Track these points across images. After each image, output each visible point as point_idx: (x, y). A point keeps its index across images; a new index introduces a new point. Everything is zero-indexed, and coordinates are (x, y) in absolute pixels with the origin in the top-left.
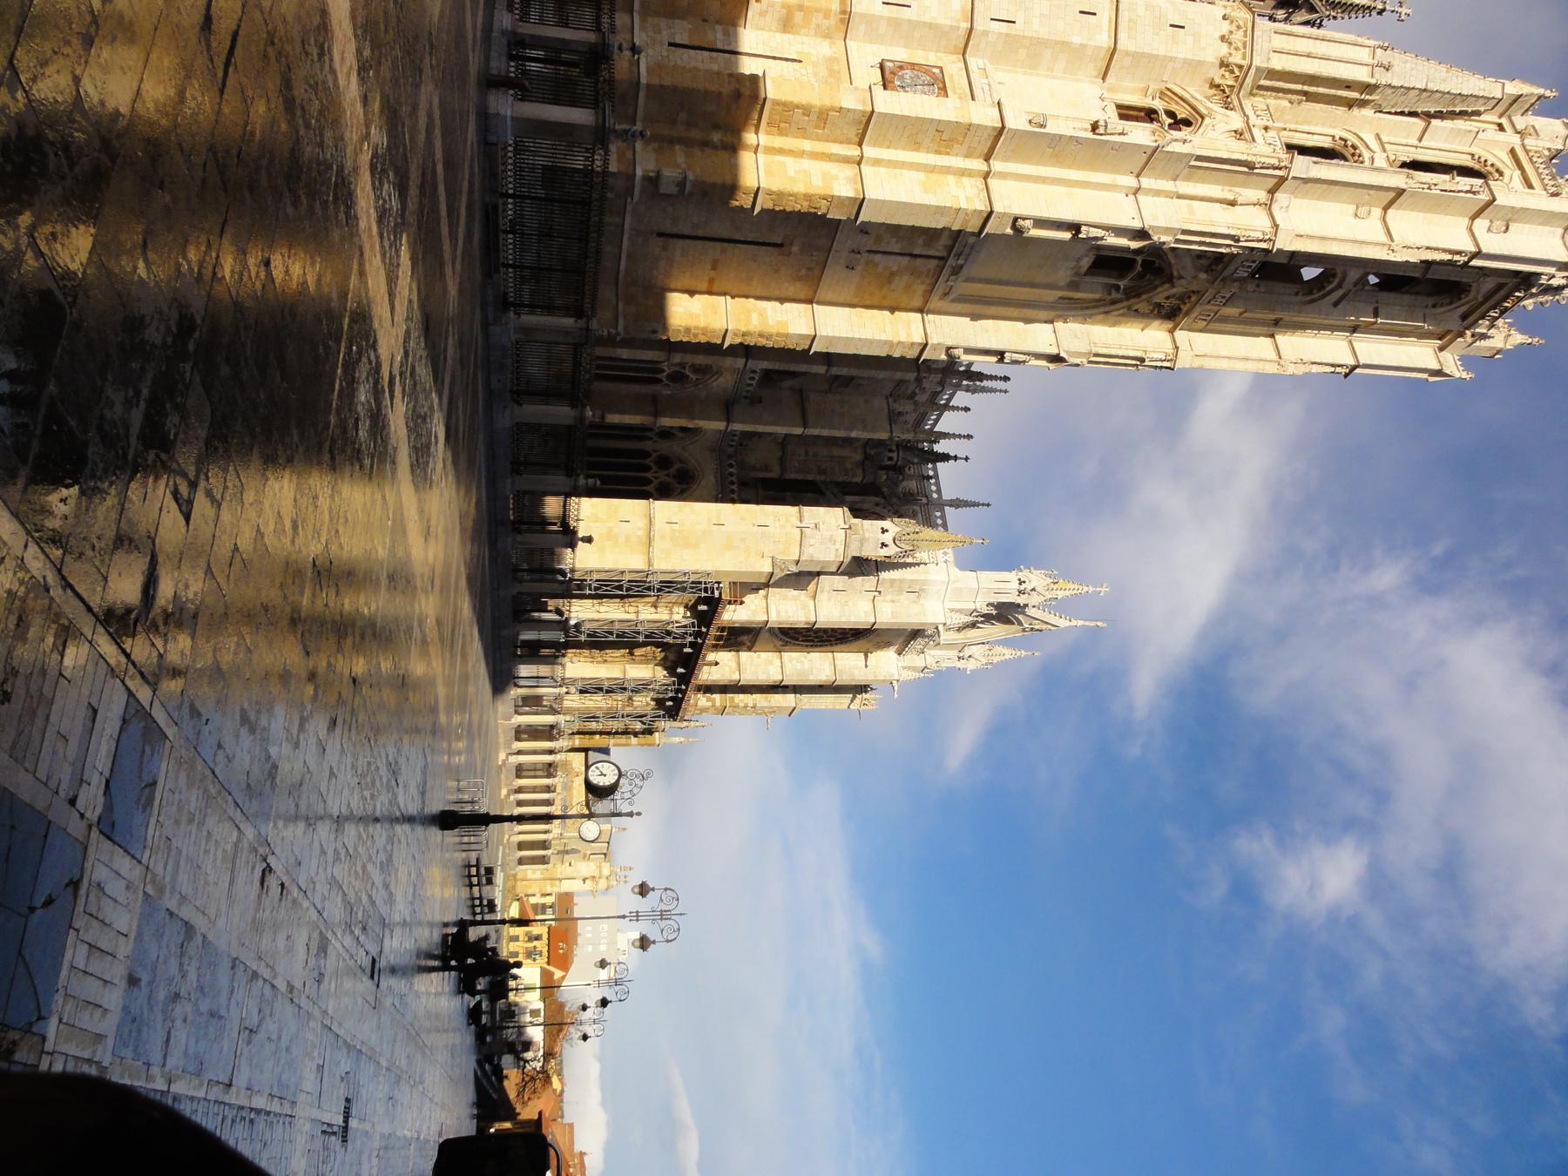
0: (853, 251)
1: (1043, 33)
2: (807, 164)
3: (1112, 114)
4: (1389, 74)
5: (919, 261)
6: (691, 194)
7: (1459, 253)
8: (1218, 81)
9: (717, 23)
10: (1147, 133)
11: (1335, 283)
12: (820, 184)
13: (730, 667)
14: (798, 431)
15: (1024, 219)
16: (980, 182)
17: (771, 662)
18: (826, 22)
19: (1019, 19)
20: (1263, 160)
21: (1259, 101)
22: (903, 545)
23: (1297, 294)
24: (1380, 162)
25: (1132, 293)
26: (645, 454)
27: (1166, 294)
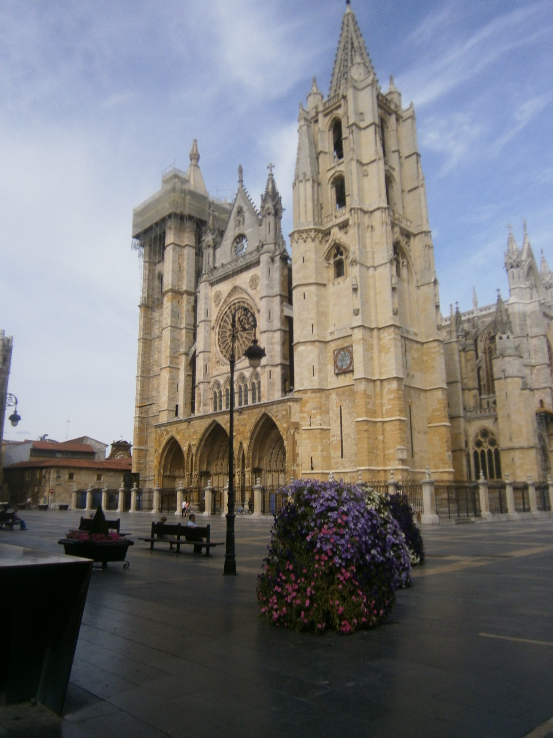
2: (385, 401)
3: (340, 279)
6: (404, 446)
8: (320, 239)
9: (329, 439)
10: (353, 267)
11: (388, 173)
12: (393, 395)
14: (460, 385)
15: (394, 311)
16: (382, 331)
18: (324, 397)
19: (310, 322)
20: (356, 219)
21: (325, 220)
25: (404, 255)
26: (476, 453)
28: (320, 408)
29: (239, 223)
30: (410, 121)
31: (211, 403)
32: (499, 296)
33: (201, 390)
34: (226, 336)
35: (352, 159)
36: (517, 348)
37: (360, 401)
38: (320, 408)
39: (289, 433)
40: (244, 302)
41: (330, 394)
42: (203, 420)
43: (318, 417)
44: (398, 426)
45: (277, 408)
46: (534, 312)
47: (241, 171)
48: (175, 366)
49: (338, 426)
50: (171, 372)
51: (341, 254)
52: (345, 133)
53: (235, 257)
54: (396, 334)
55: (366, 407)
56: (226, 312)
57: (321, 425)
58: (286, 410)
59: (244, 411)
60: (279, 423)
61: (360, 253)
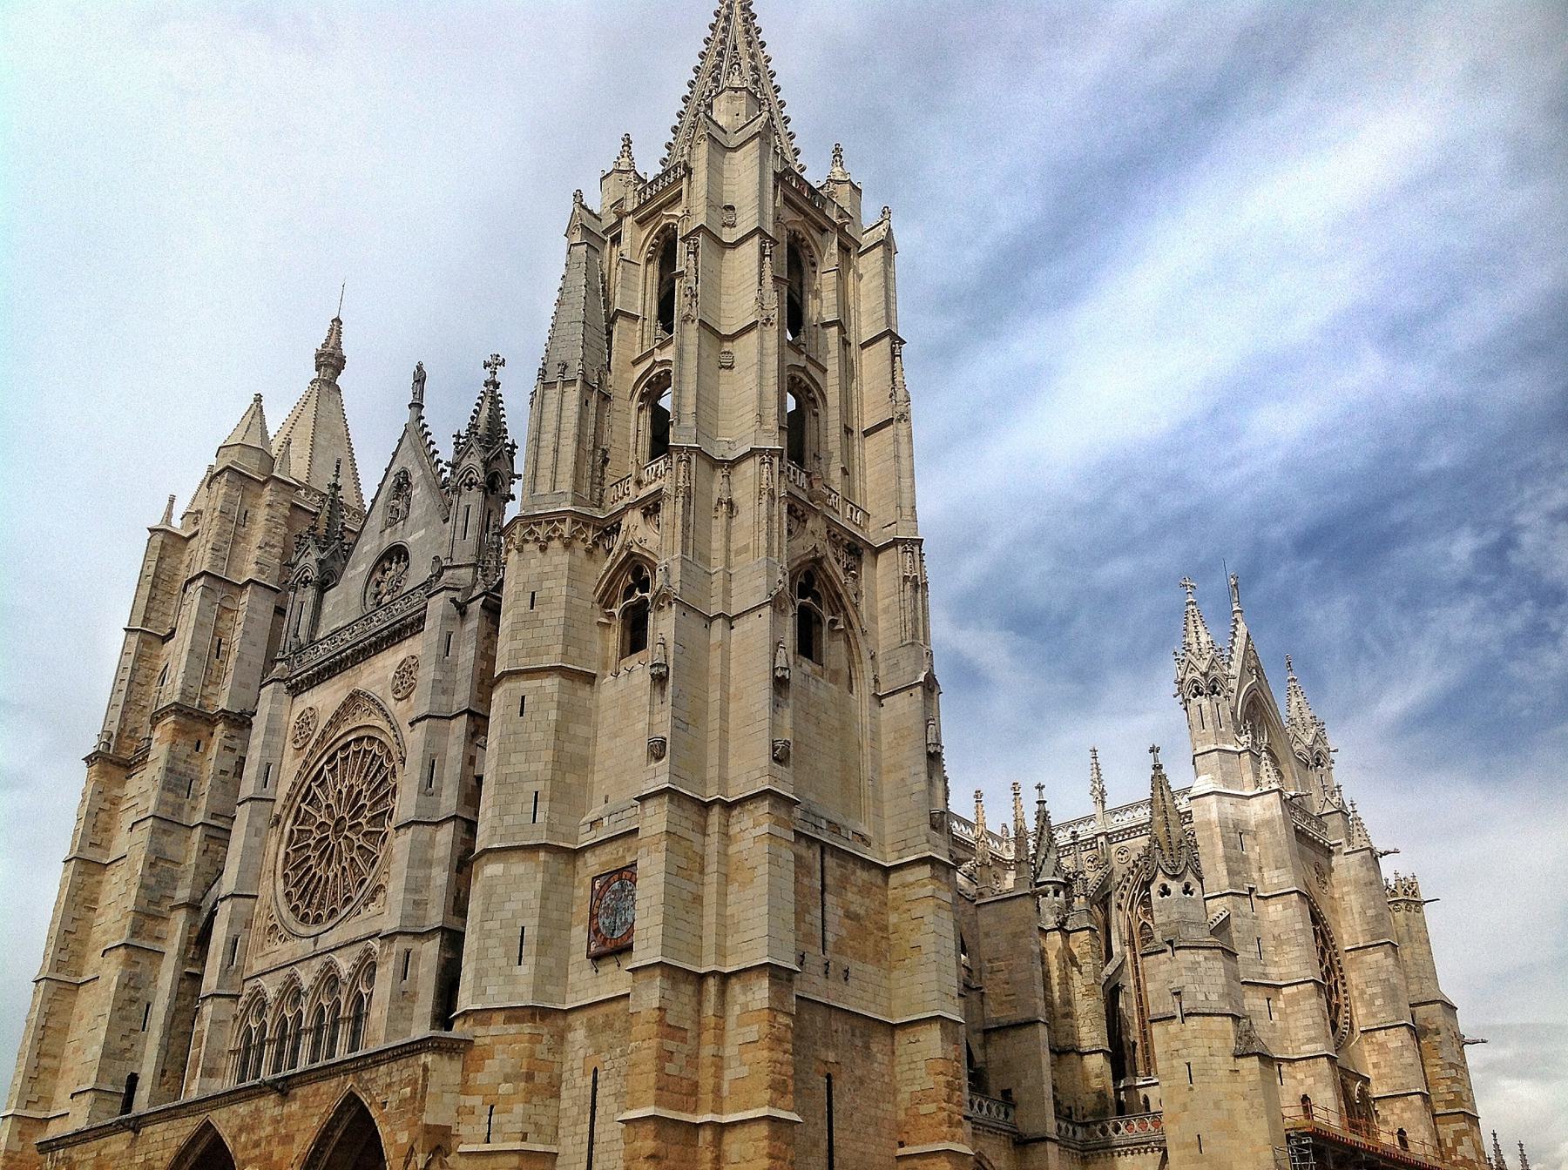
0: (826, 973)
1: (548, 755)
2: (730, 1051)
4: (570, 363)
5: (829, 880)
7: (762, 250)
11: (802, 375)
13: (1403, 1110)
14: (1043, 1032)
15: (774, 750)
17: (1382, 1045)
18: (544, 1042)
19: (530, 787)
20: (681, 479)
21: (611, 494)
22: (1183, 863)
23: (816, 415)
24: (669, 354)
27: (833, 561)
28: (529, 1077)
29: (396, 516)
30: (879, 251)
31: (230, 1064)
32: (1155, 767)
33: (203, 1026)
34: (309, 845)
35: (686, 319)
36: (1223, 927)
37: (644, 1043)
38: (529, 1077)
39: (411, 1166)
40: (371, 739)
41: (569, 1028)
42: (177, 1123)
43: (518, 1108)
44: (766, 1143)
45: (390, 1074)
46: (1268, 823)
47: (420, 378)
48: (146, 944)
49: (582, 1143)
50: (129, 963)
51: (645, 589)
52: (683, 261)
53: (370, 608)
54: (778, 822)
55: (661, 1069)
56: (322, 769)
57: (524, 1139)
58: (412, 1082)
59: (292, 1087)
60: (388, 1129)
61: (685, 571)
